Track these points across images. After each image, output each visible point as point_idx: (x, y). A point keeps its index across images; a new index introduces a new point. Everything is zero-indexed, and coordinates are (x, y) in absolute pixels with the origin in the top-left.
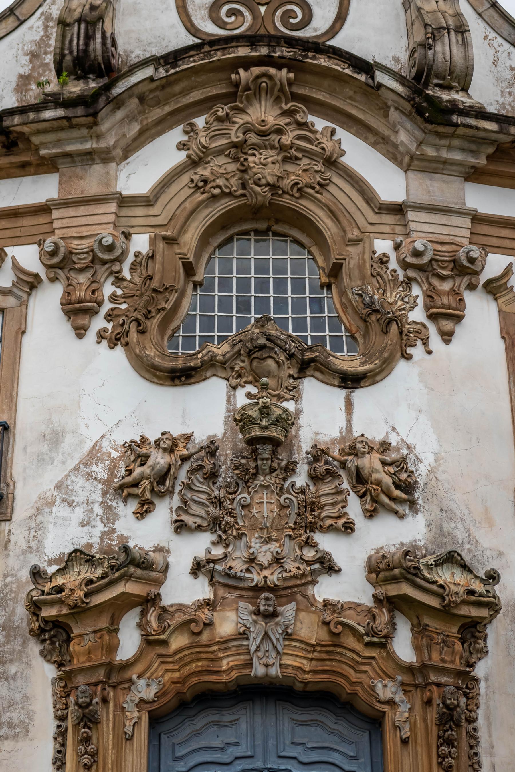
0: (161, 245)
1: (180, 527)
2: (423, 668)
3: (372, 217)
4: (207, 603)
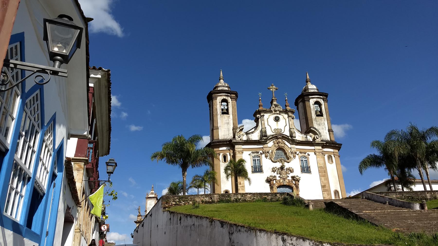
1: (277, 174)
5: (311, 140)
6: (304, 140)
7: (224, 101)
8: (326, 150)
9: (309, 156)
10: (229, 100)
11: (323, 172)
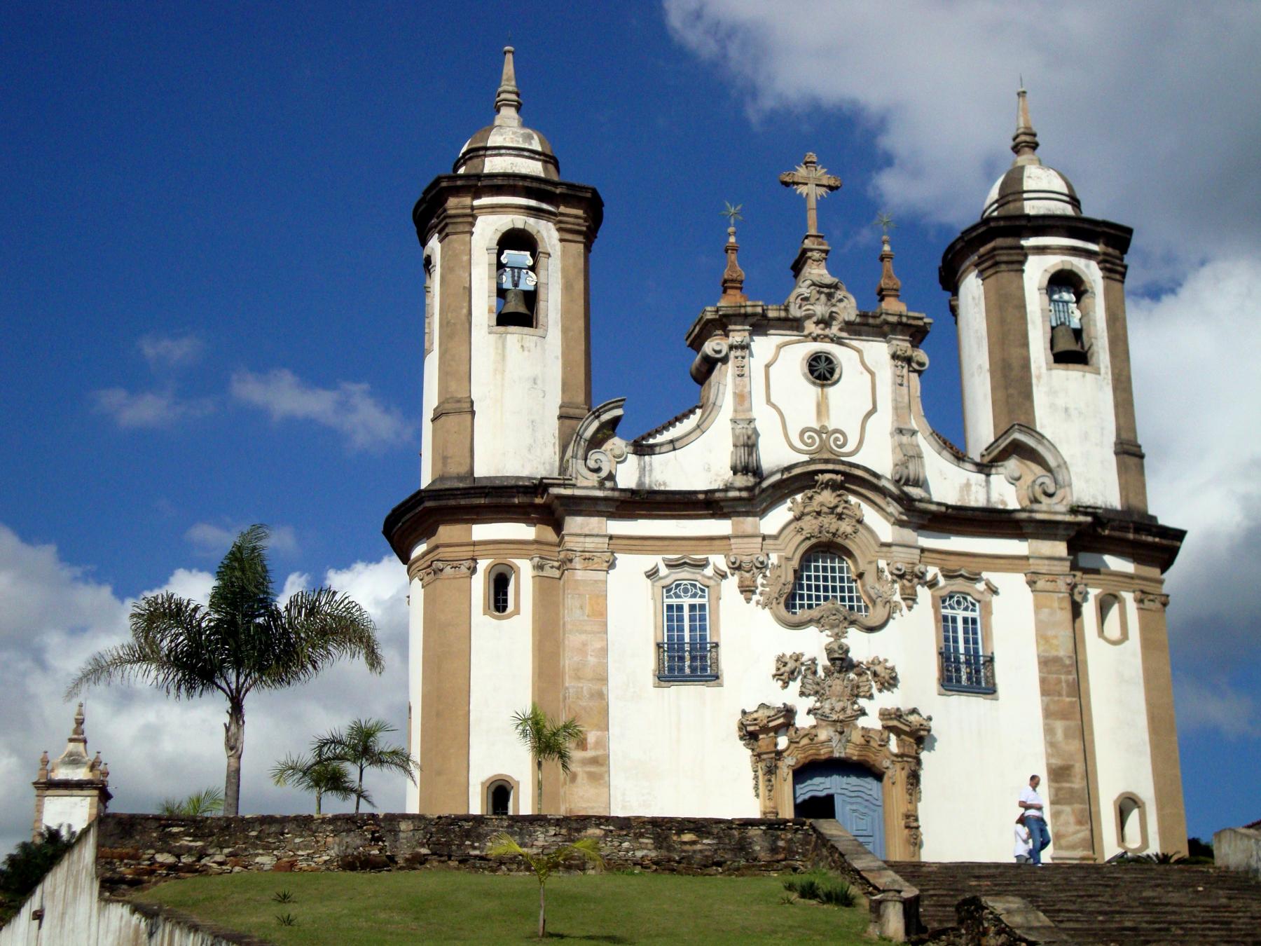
0: (783, 562)
1: (802, 694)
2: (902, 756)
3: (877, 549)
4: (815, 727)
5: (1013, 504)
6: (977, 499)
7: (515, 239)
8: (1086, 559)
9: (995, 598)
10: (547, 233)
11: (1066, 687)
